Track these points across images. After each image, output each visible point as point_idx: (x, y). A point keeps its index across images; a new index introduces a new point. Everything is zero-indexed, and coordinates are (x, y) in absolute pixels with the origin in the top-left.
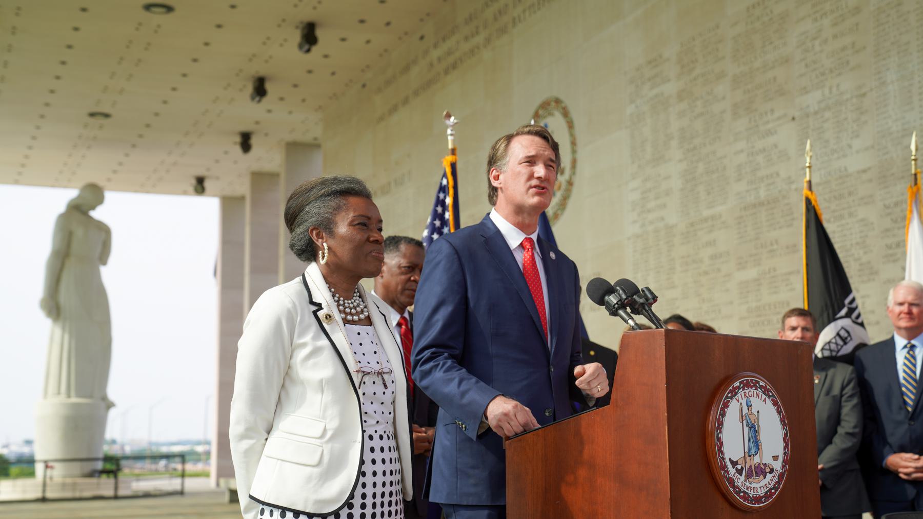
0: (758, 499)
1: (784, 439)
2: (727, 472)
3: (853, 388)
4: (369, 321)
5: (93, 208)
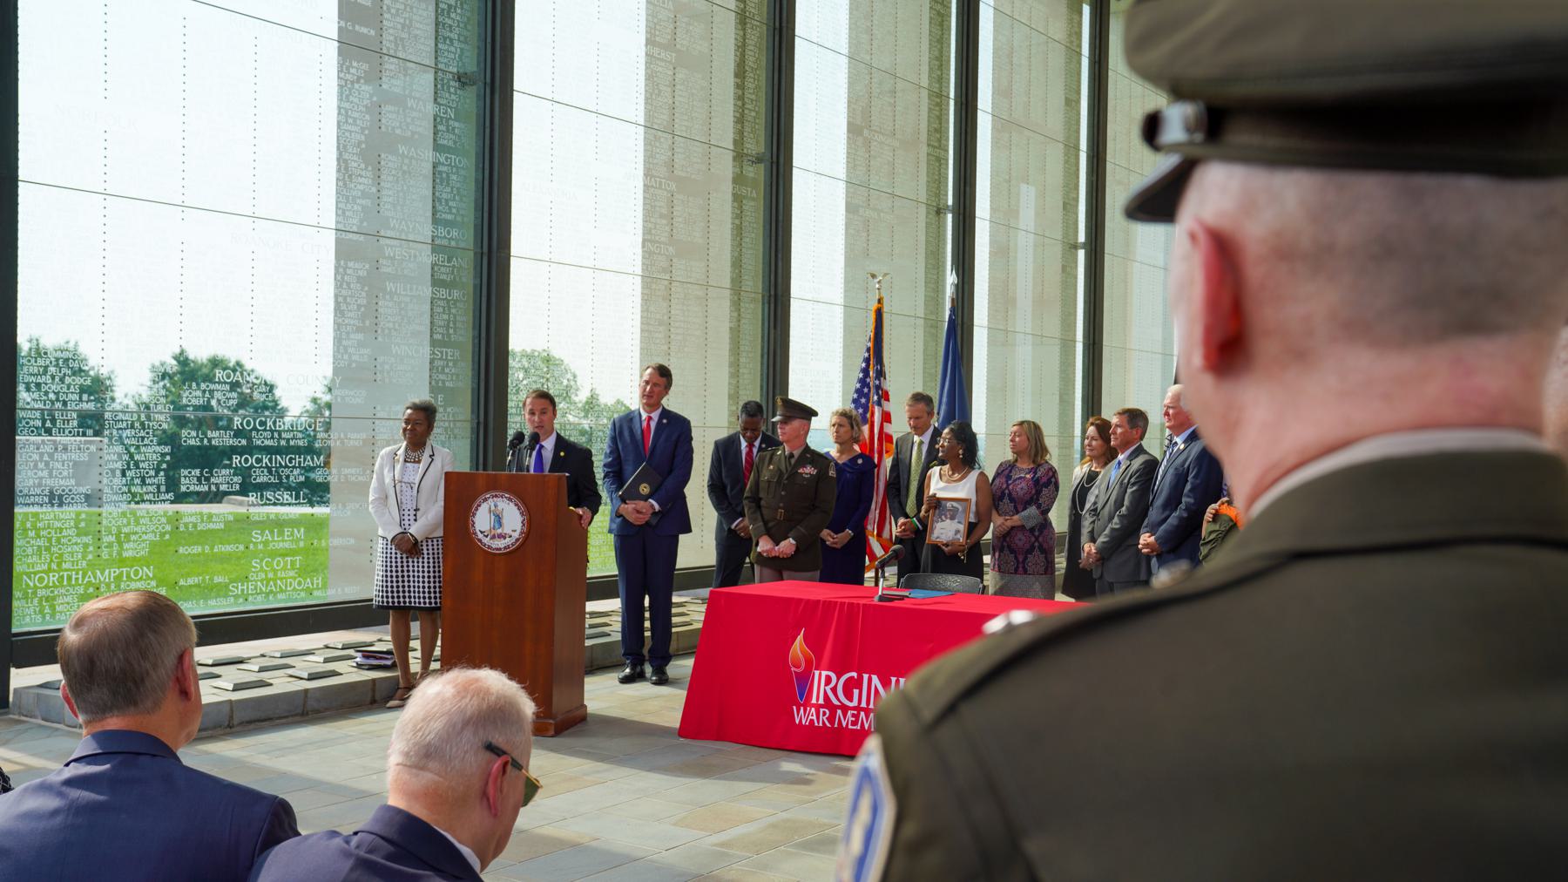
1: (522, 522)
3: (1136, 479)
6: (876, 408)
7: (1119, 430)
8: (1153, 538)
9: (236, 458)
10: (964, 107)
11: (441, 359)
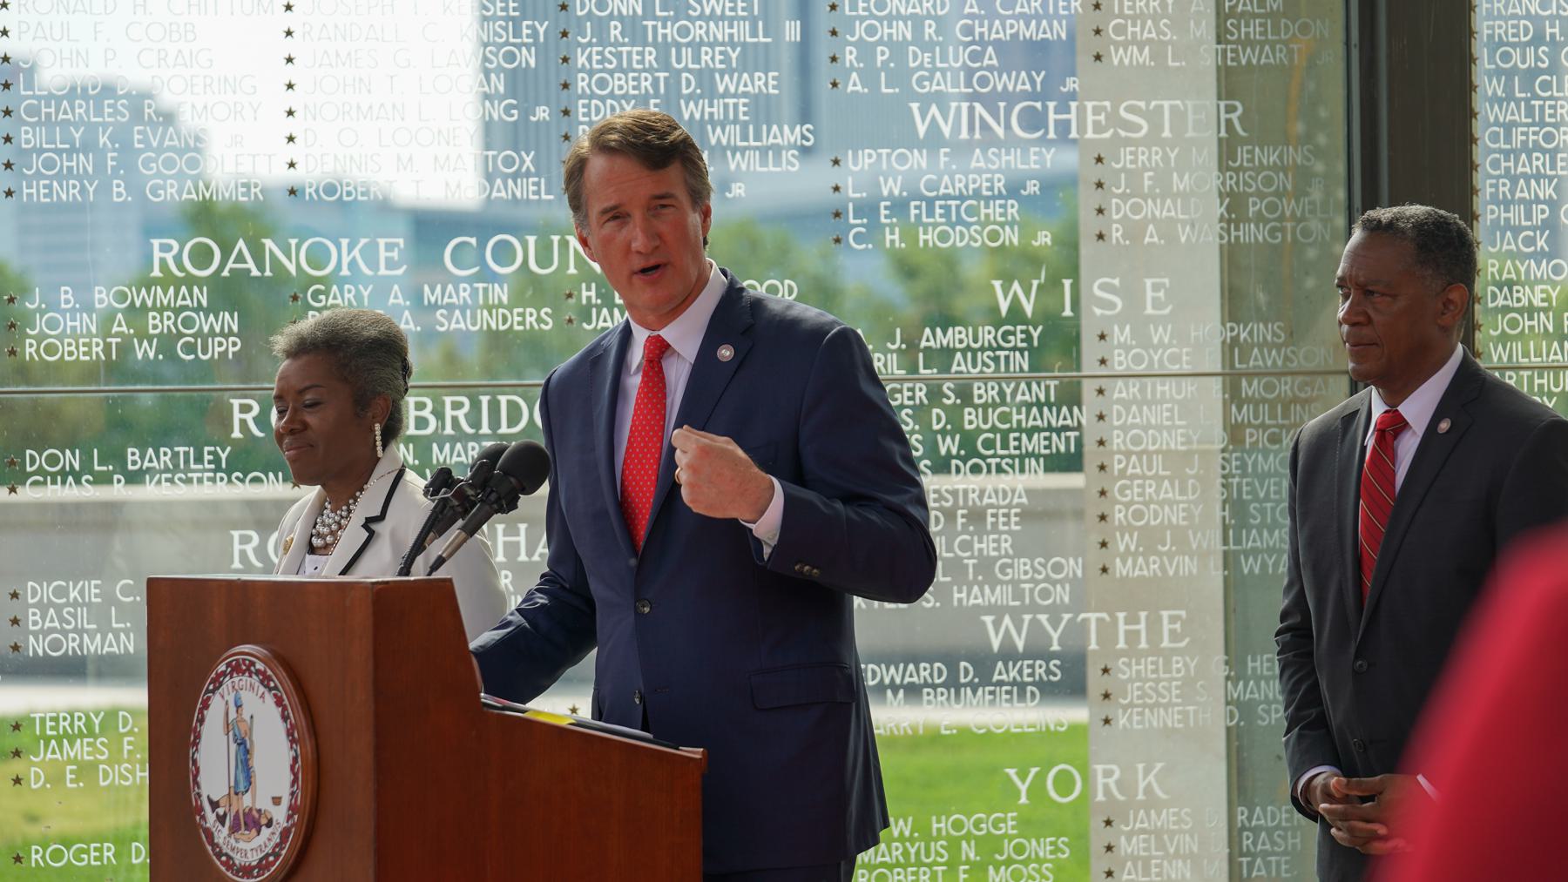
0: (247, 871)
1: (292, 768)
2: (203, 818)
9: (245, 540)
11: (1153, 139)
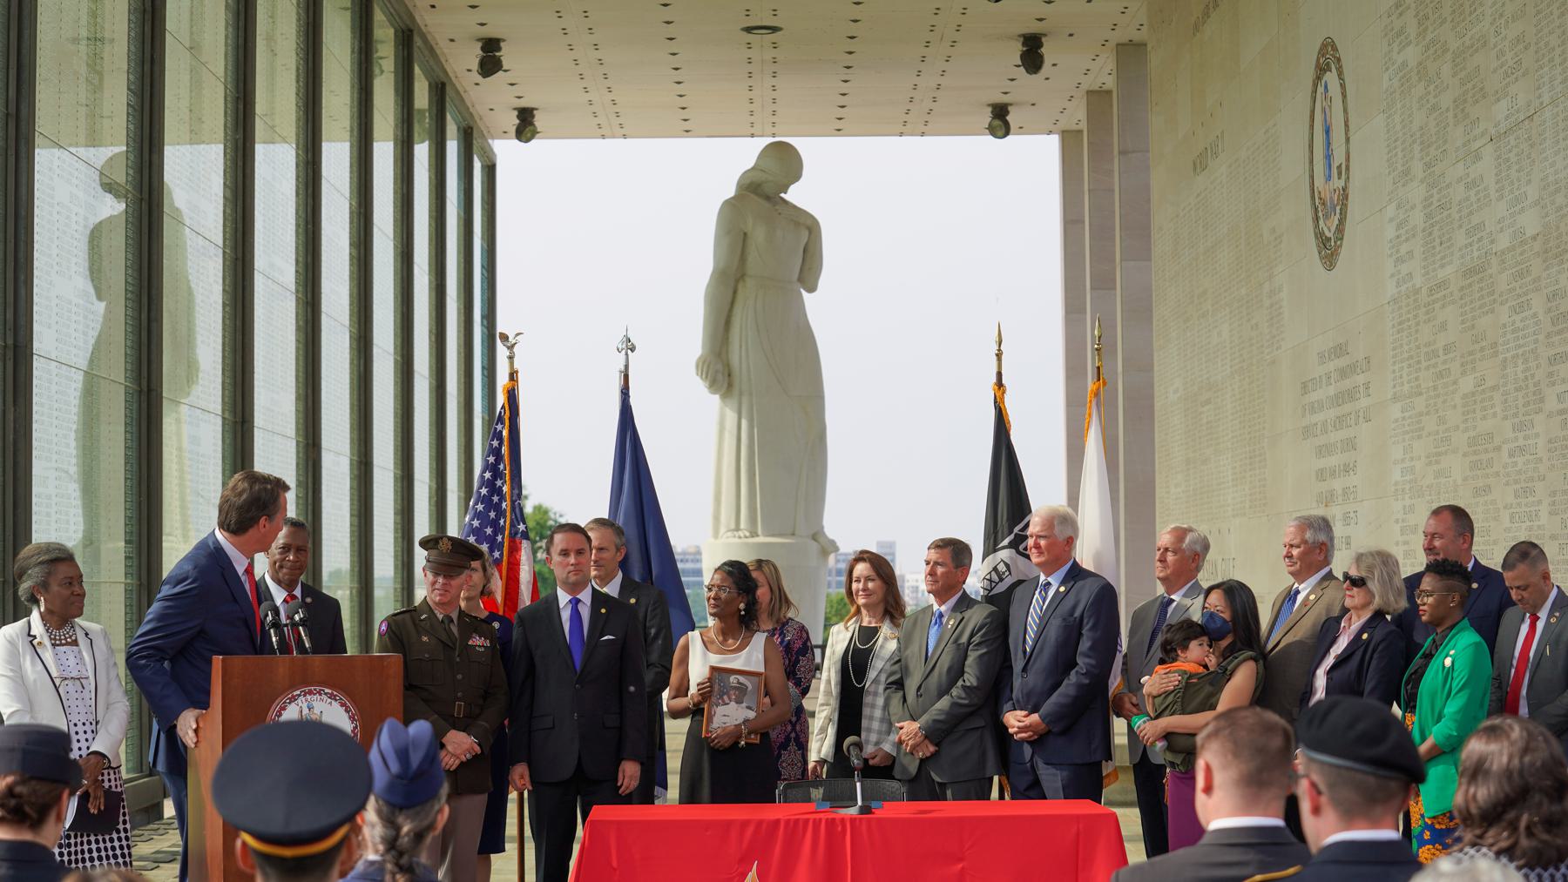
4: (75, 643)
5: (785, 190)
6: (525, 544)
7: (940, 570)
8: (1035, 717)
10: (148, 17)
